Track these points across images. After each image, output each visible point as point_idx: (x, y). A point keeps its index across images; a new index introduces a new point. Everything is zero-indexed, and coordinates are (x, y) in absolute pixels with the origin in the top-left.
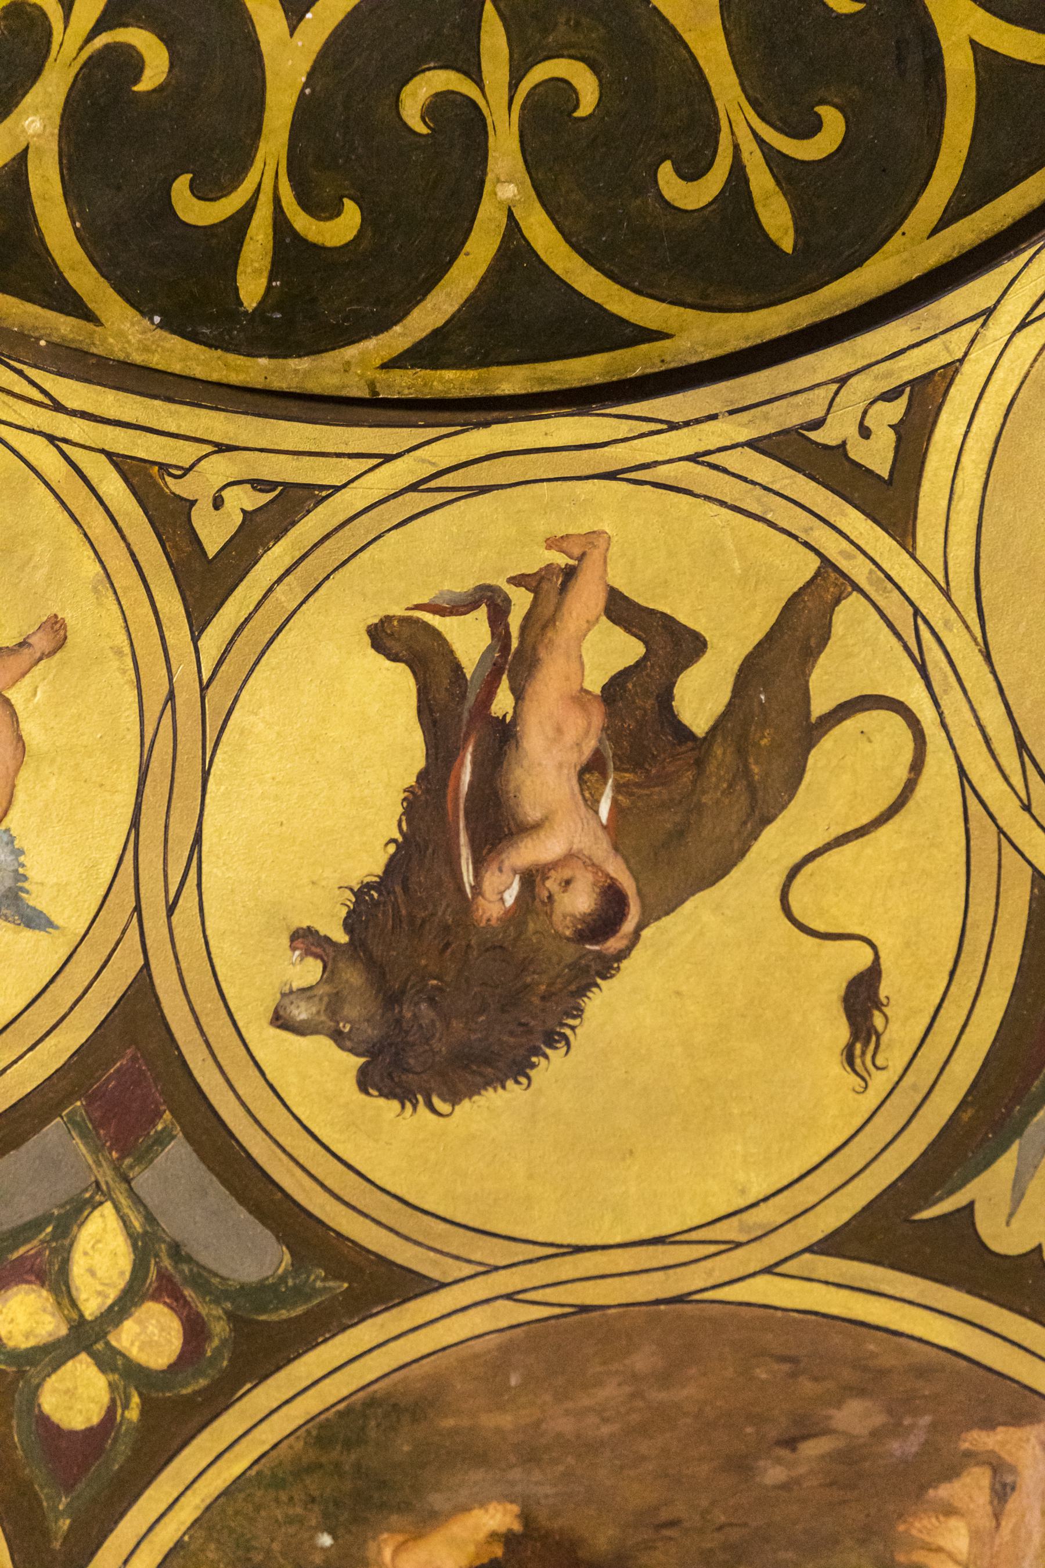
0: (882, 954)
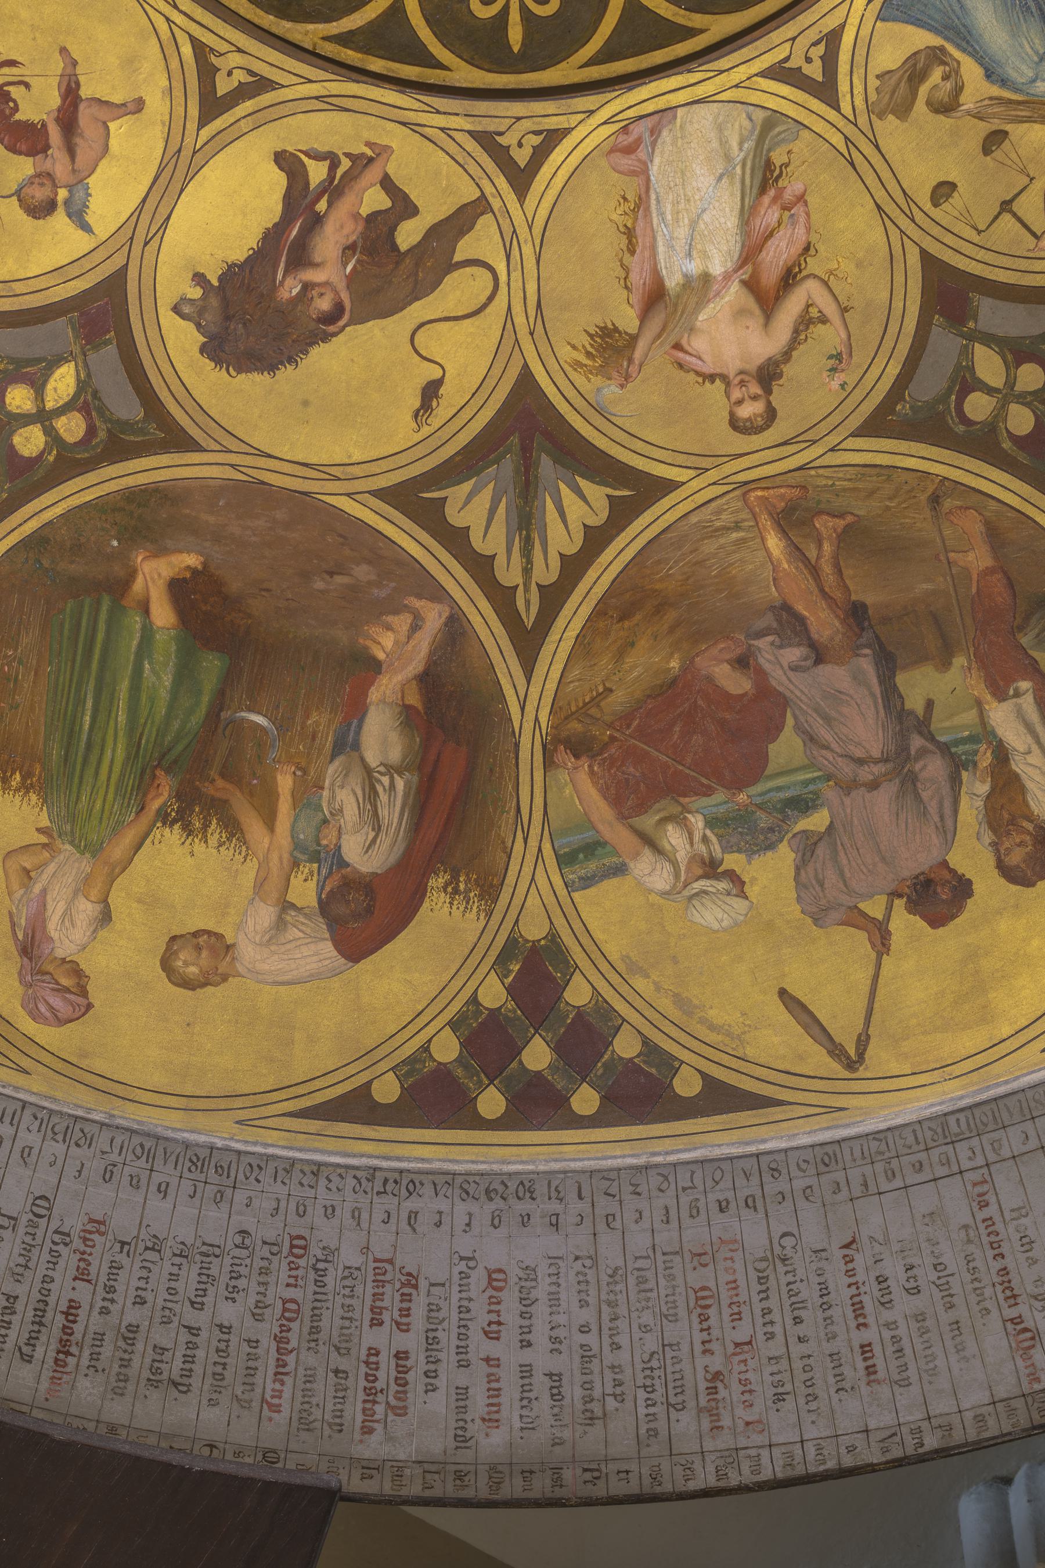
0: (447, 375)
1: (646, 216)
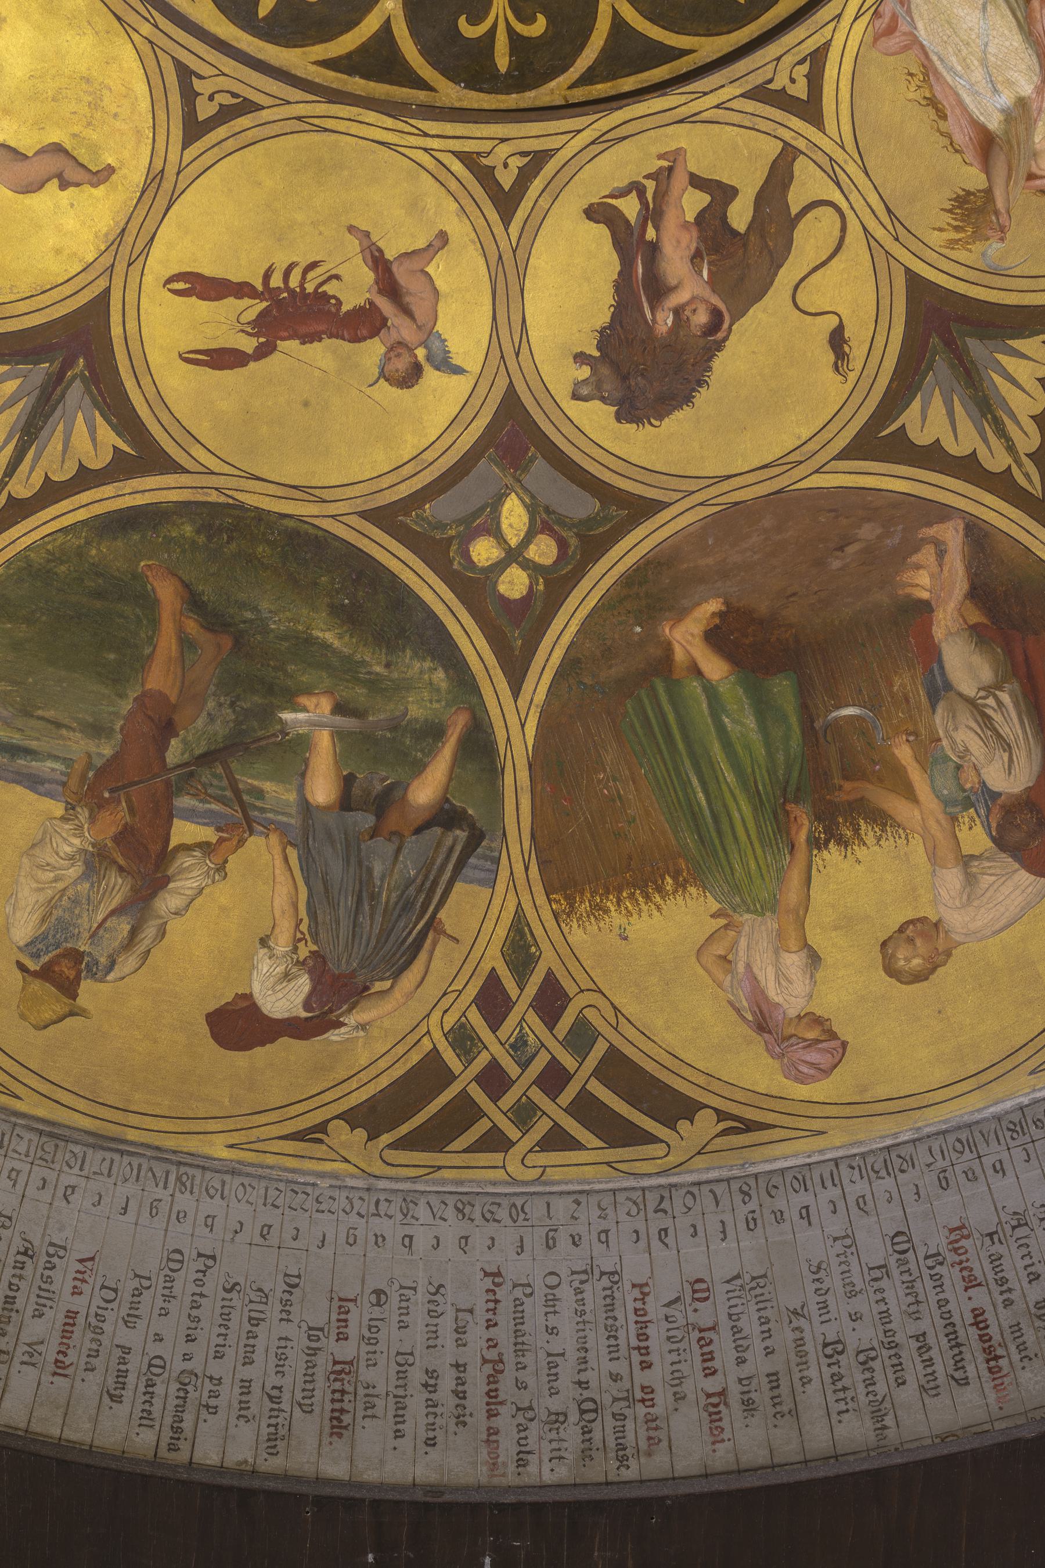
1: (938, 79)
